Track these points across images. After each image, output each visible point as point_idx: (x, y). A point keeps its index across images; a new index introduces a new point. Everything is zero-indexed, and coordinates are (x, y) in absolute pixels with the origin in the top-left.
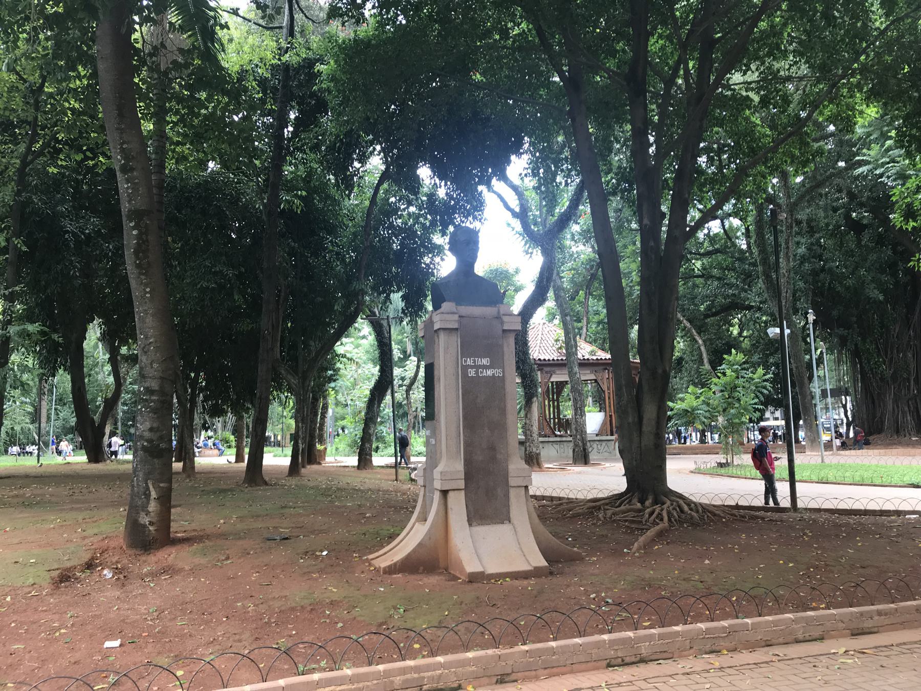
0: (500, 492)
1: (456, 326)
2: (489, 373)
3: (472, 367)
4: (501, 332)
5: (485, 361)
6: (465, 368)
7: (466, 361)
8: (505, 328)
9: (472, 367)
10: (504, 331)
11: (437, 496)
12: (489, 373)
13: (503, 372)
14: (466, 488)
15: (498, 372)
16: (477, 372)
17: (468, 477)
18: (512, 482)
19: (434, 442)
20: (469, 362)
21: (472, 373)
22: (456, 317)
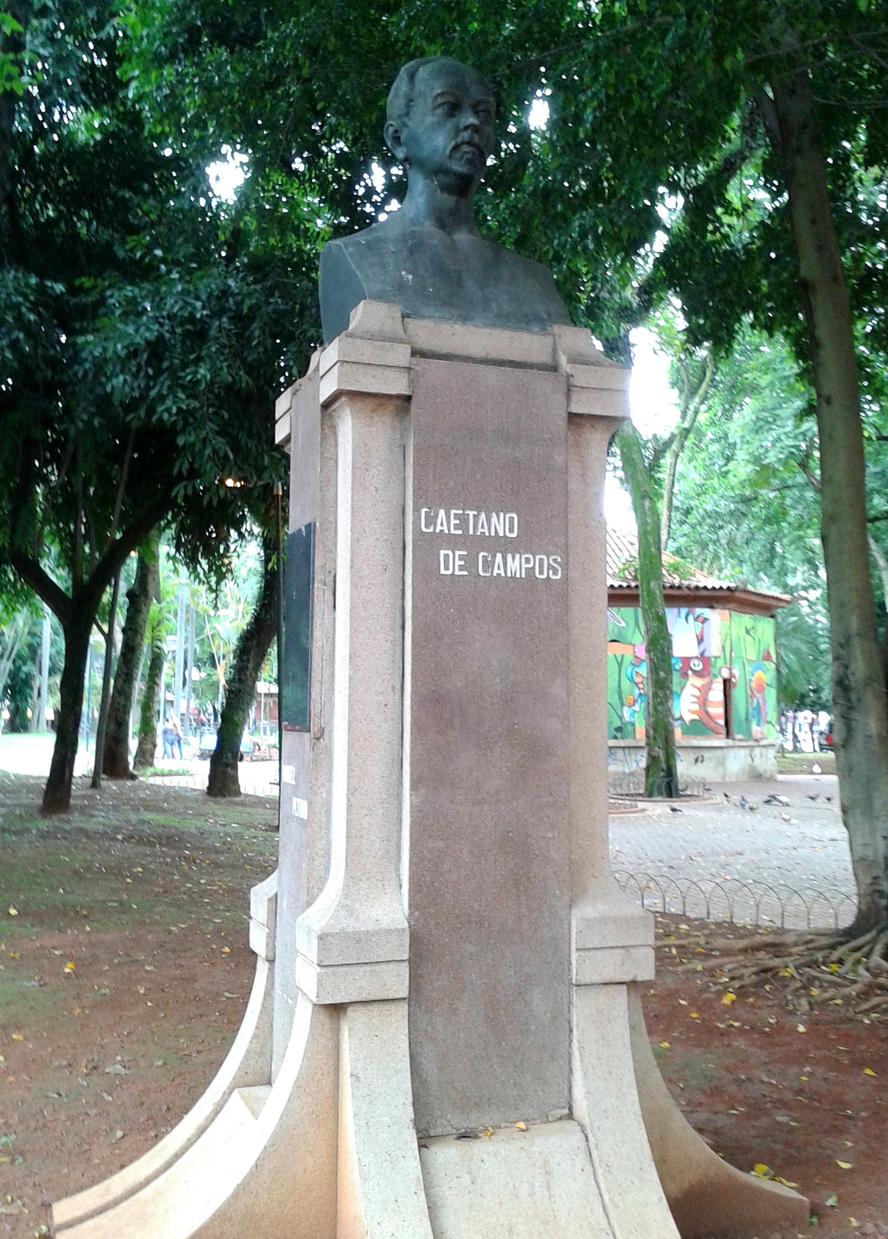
0: (538, 1001)
1: (398, 386)
2: (516, 566)
3: (452, 542)
4: (561, 422)
5: (502, 524)
6: (429, 544)
7: (431, 520)
8: (576, 409)
9: (452, 542)
10: (574, 419)
11: (304, 1015)
12: (516, 566)
13: (565, 566)
14: (416, 996)
15: (545, 566)
16: (470, 562)
17: (421, 952)
18: (582, 967)
19: (303, 813)
20: (445, 522)
21: (452, 563)
22: (401, 355)
